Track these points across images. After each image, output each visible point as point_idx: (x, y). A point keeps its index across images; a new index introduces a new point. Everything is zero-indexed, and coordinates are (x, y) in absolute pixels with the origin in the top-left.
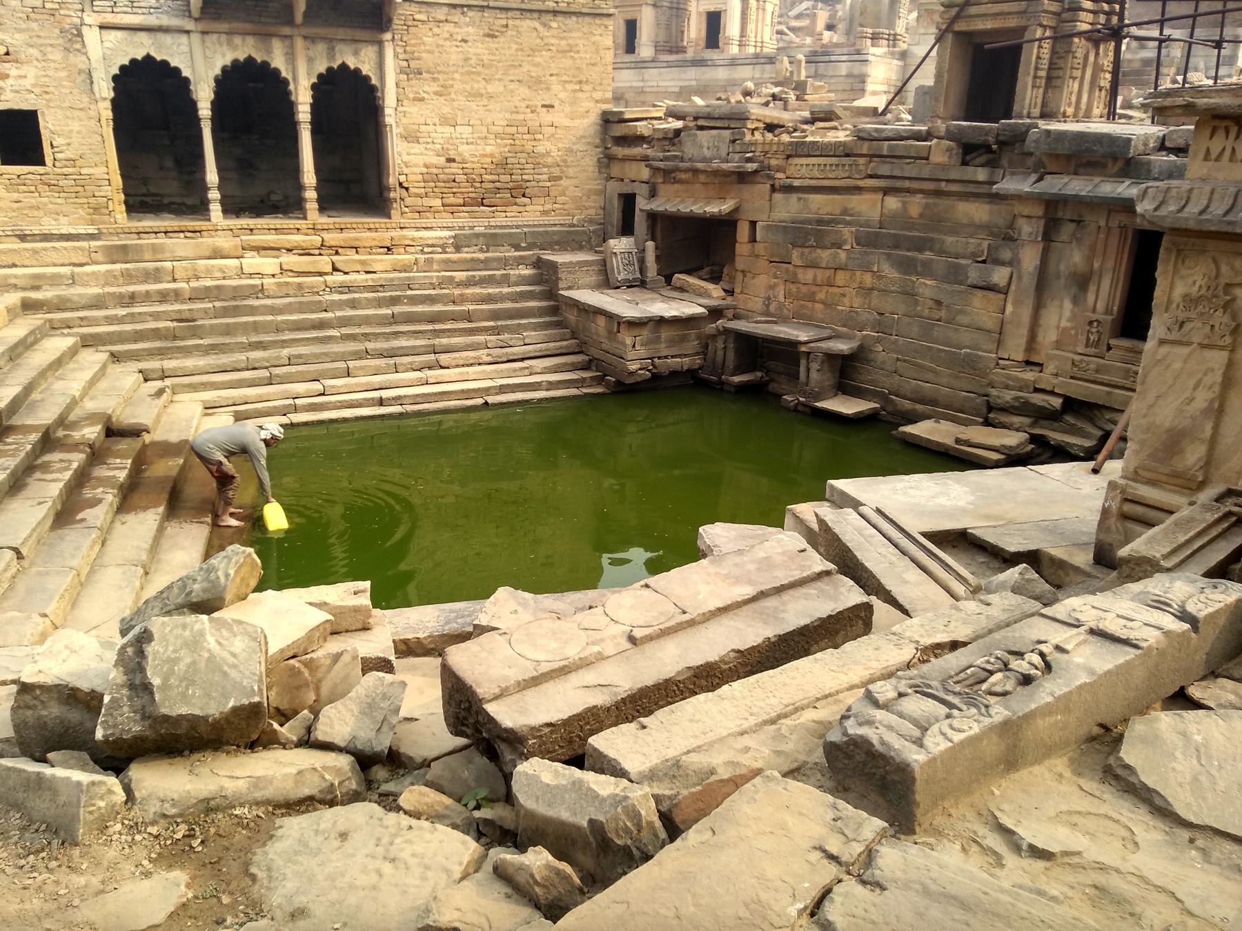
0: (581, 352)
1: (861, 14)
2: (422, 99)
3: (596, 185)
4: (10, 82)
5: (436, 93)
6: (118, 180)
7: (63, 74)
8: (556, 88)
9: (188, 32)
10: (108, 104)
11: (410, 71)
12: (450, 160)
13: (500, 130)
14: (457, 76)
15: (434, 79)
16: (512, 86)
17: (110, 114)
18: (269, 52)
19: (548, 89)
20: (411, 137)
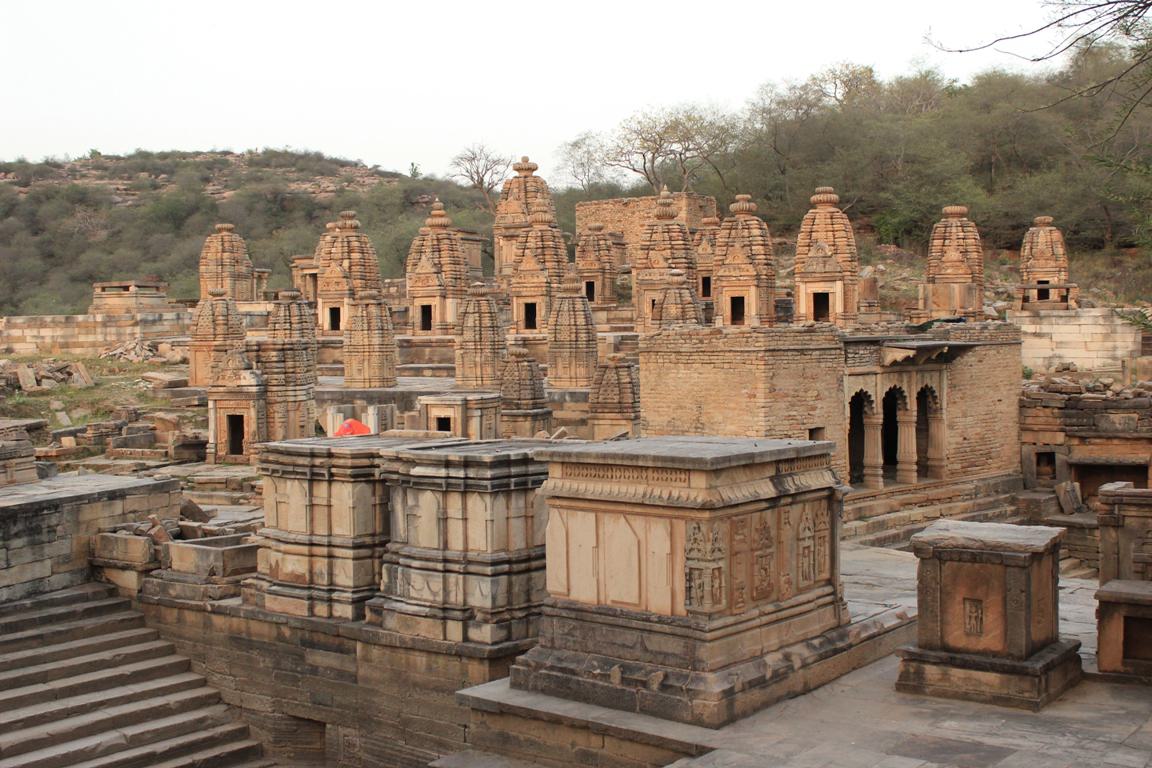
0: (1070, 557)
1: (934, 295)
2: (955, 403)
3: (1016, 448)
4: (818, 411)
5: (962, 398)
6: (848, 468)
7: (836, 404)
8: (1002, 388)
9: (876, 374)
10: (848, 421)
11: (952, 387)
12: (965, 439)
13: (983, 417)
14: (968, 387)
15: (960, 390)
16: (987, 390)
17: (848, 427)
18: (902, 381)
19: (999, 390)
20: (951, 427)
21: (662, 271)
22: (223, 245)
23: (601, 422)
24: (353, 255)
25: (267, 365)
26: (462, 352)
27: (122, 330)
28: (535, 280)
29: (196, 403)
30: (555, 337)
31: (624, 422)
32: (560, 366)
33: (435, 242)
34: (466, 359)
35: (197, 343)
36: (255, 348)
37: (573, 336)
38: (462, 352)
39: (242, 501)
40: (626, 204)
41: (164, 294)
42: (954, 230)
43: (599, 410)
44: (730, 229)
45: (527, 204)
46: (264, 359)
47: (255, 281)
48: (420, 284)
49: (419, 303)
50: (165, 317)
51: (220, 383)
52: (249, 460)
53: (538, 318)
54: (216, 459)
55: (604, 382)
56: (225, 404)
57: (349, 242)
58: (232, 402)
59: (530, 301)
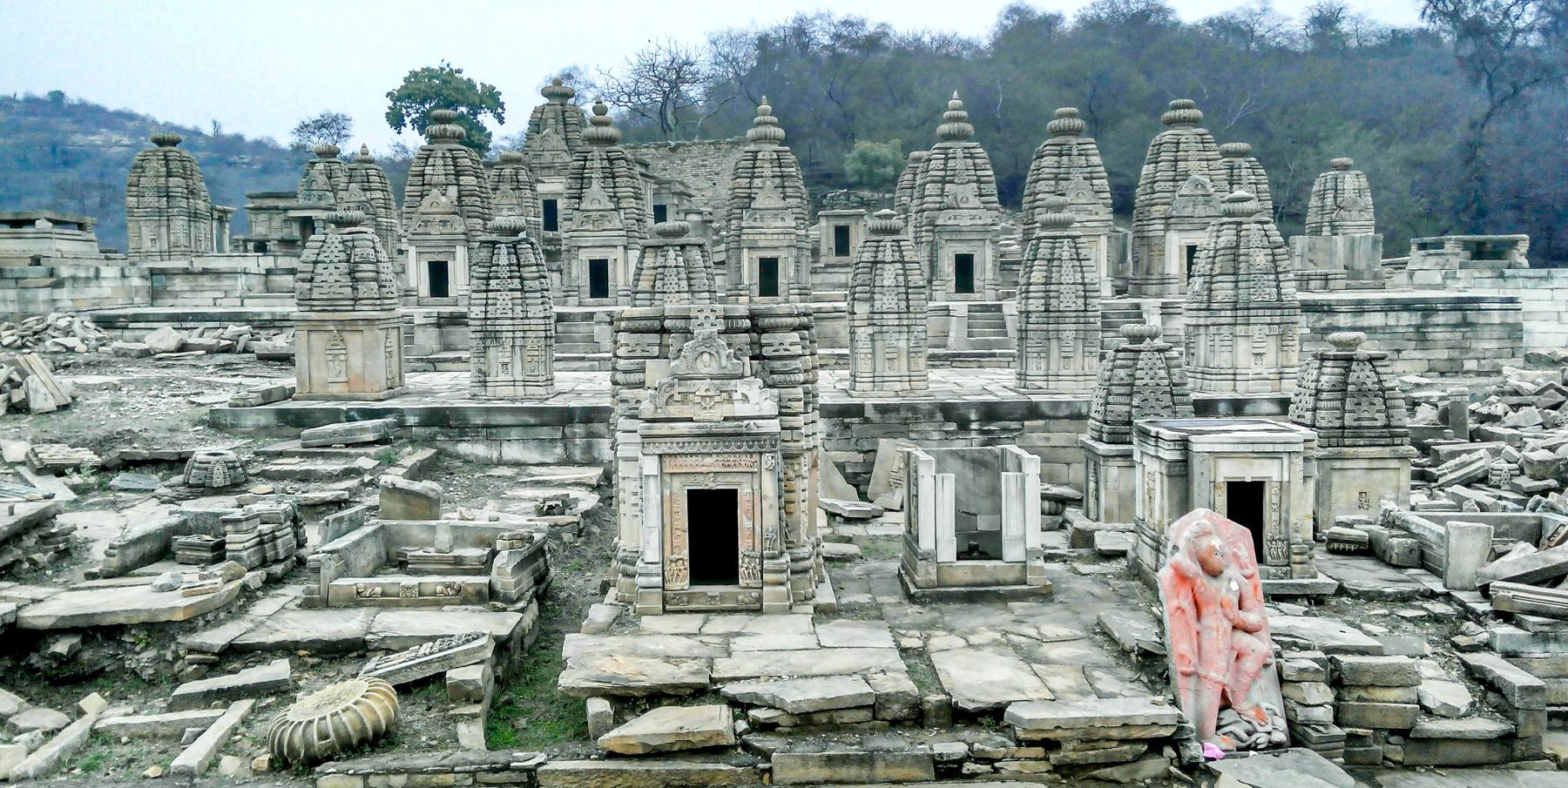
21: (974, 212)
22: (167, 165)
23: (1347, 464)
24: (464, 180)
25: (777, 364)
26: (870, 330)
27: (29, 294)
28: (779, 223)
29: (370, 437)
30: (1047, 305)
31: (1394, 464)
32: (1054, 354)
33: (605, 163)
34: (879, 344)
35: (313, 316)
36: (747, 323)
37: (1081, 302)
38: (870, 330)
39: (969, 767)
40: (673, 150)
41: (92, 236)
42: (1244, 172)
43: (1347, 442)
44: (1060, 155)
45: (567, 140)
46: (767, 351)
47: (215, 224)
48: (590, 227)
49: (586, 256)
50: (102, 274)
51: (674, 411)
52: (760, 599)
53: (781, 280)
54: (665, 602)
55: (1350, 388)
56: (690, 464)
57: (454, 158)
58: (708, 460)
59: (769, 254)
